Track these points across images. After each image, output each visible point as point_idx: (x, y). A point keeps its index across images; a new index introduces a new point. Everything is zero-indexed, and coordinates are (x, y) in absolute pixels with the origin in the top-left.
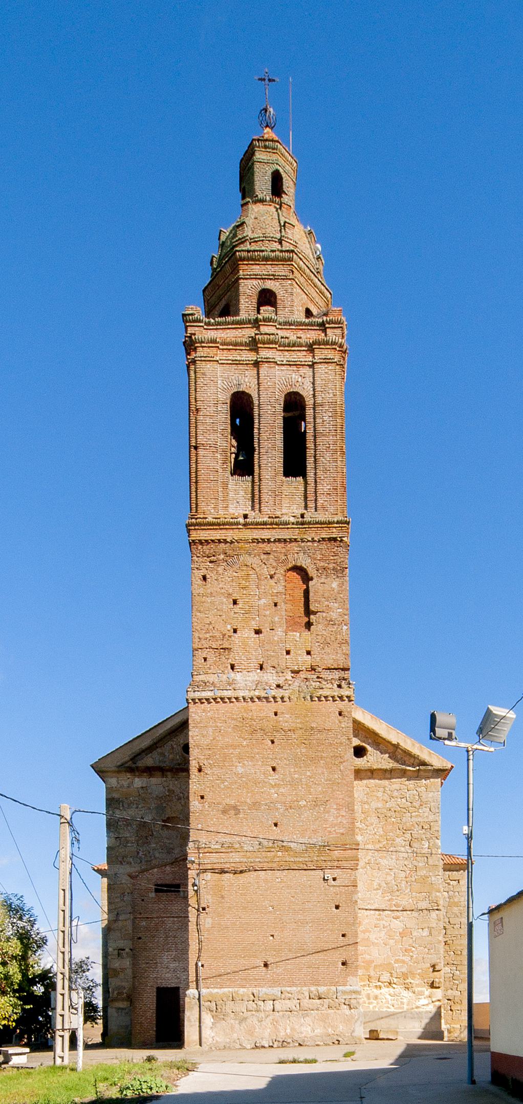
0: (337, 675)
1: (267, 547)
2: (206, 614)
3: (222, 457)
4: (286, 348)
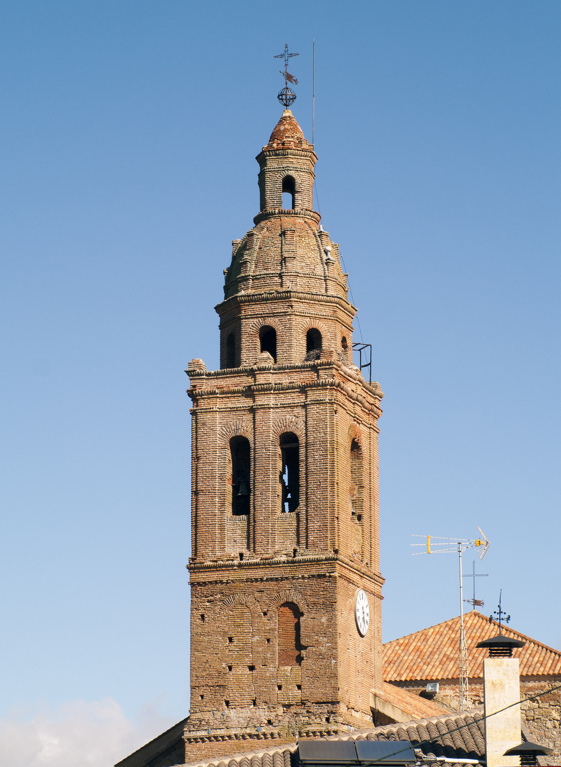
0: (326, 709)
1: (260, 585)
2: (203, 653)
3: (220, 500)
4: (281, 392)
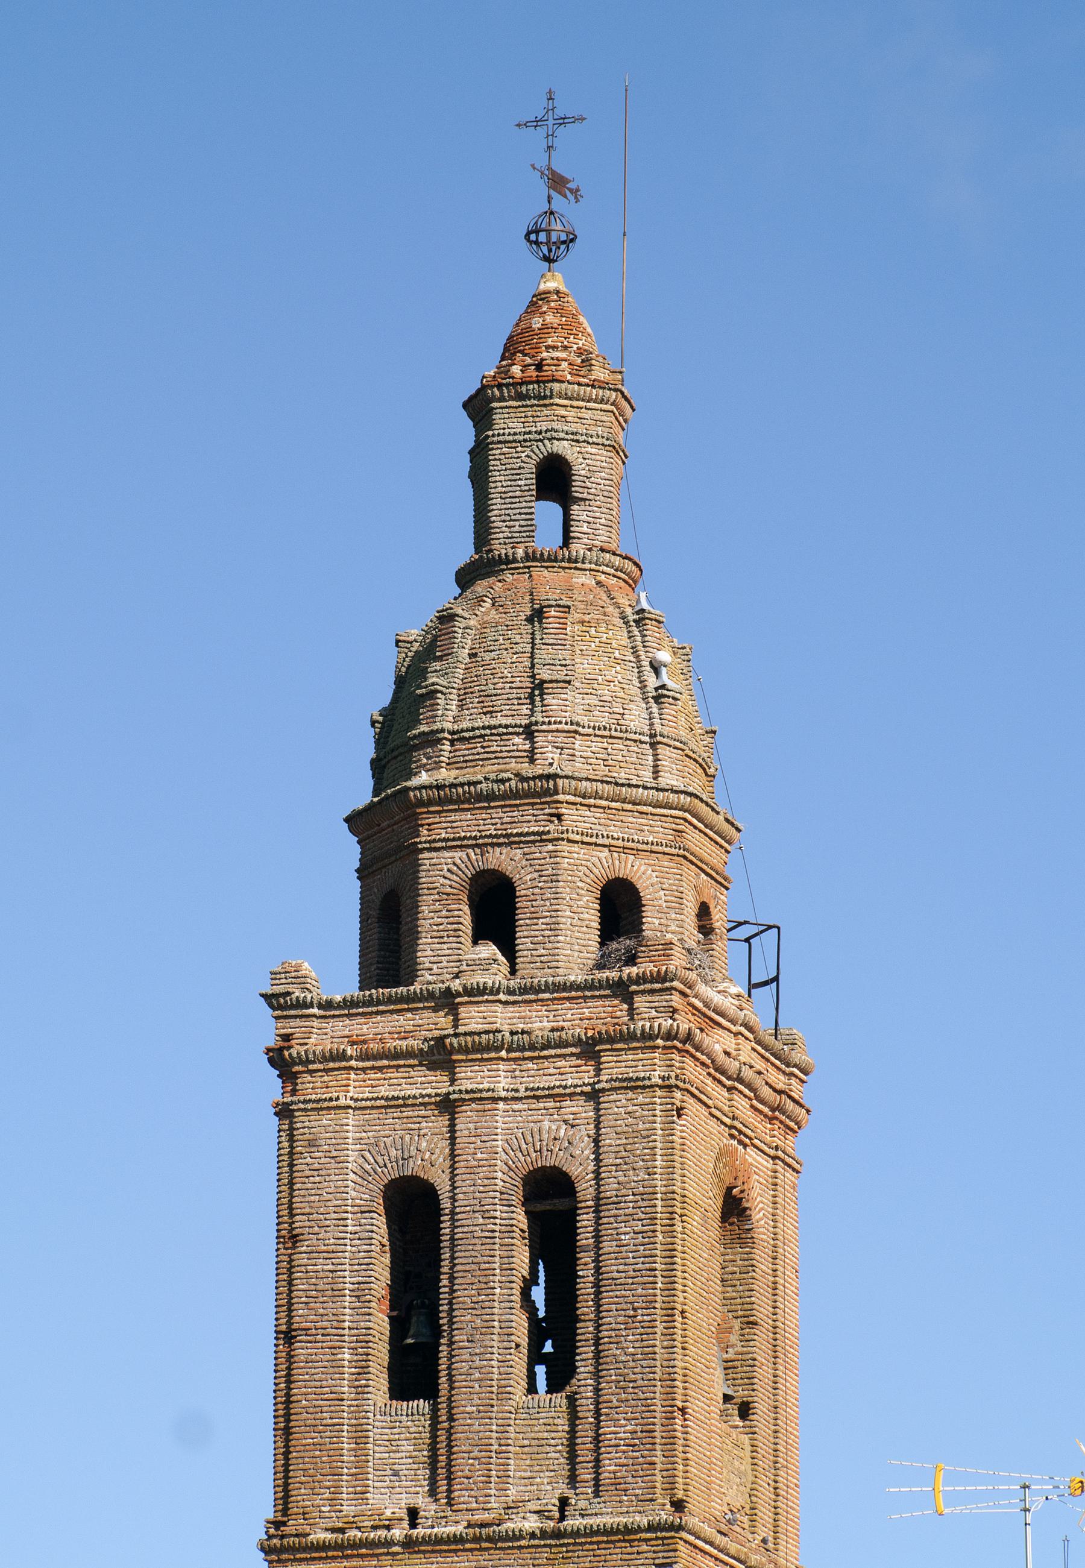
3: (355, 1358)
4: (528, 1054)
